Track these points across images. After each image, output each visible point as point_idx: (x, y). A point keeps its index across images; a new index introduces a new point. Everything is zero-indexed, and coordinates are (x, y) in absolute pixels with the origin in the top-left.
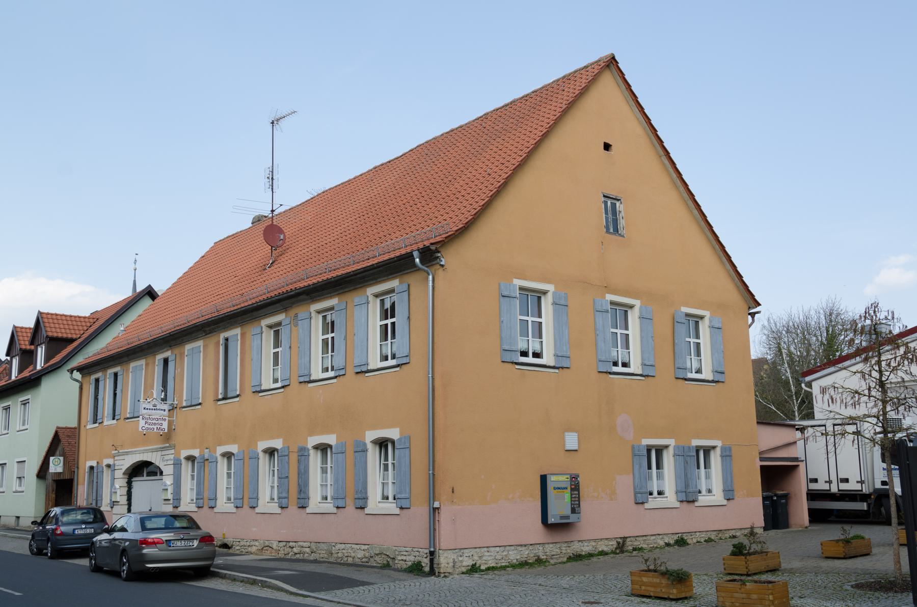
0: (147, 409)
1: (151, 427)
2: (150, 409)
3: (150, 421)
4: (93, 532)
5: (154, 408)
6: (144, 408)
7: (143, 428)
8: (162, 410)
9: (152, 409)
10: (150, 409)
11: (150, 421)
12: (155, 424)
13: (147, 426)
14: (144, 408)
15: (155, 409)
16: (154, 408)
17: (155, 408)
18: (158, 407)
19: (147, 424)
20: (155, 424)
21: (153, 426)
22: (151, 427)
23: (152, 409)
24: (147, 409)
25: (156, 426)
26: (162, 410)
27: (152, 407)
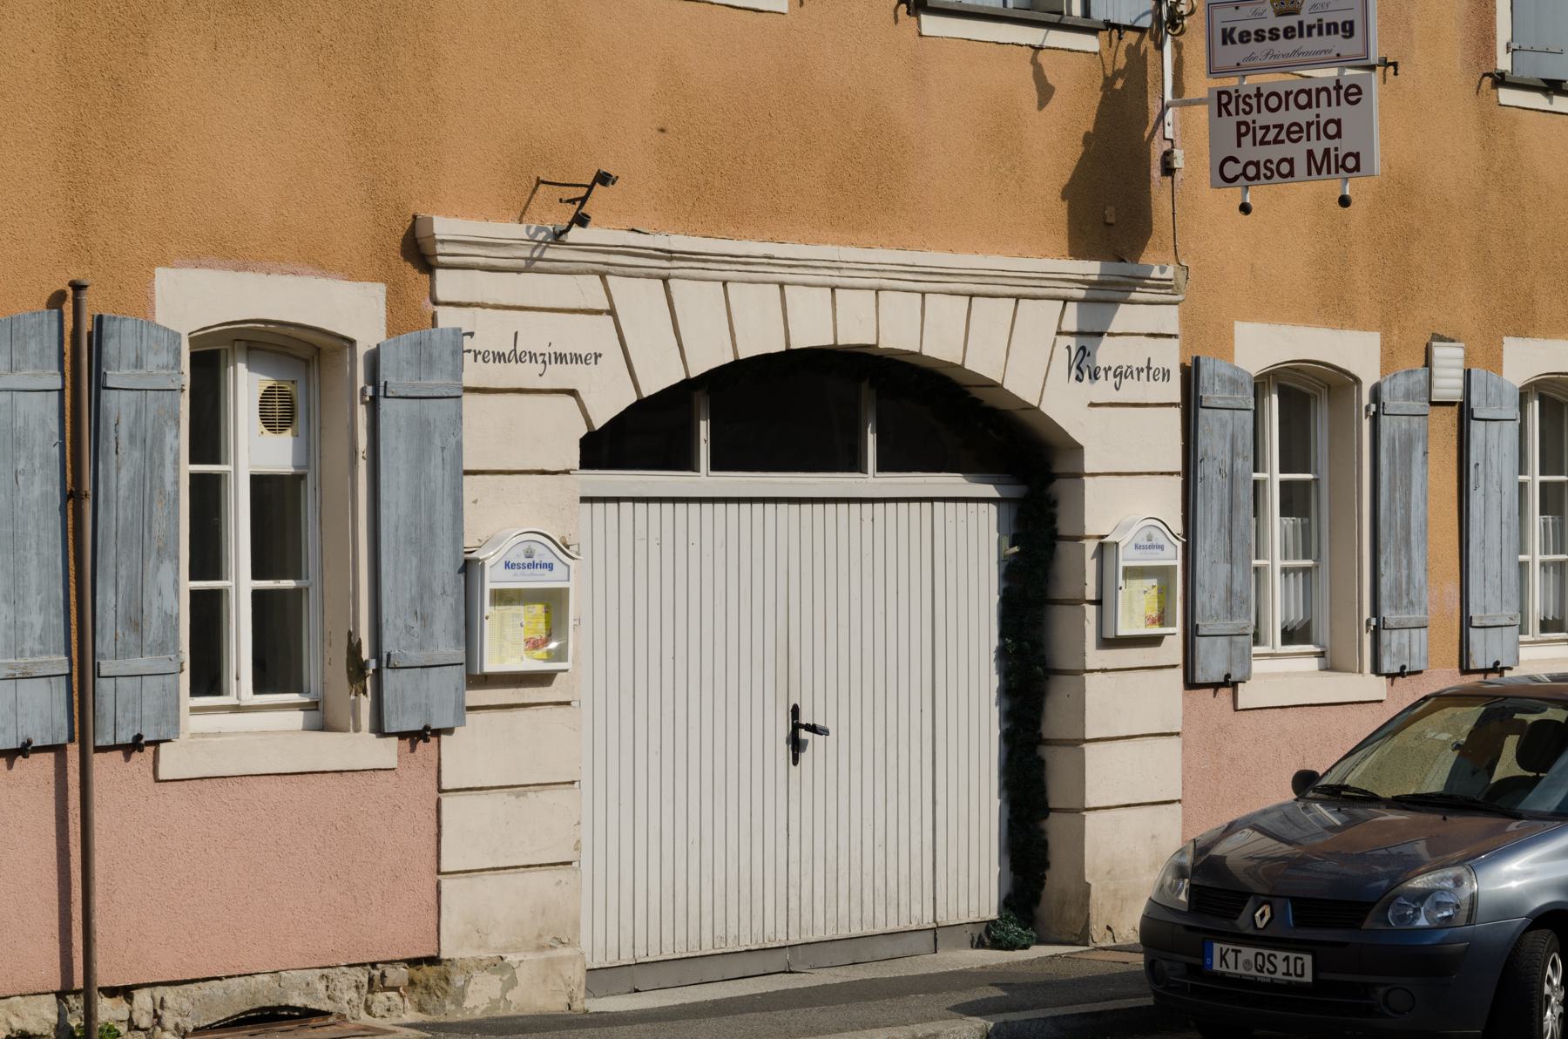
0: (1245, 37)
1: (1275, 153)
2: (1260, 35)
3: (1265, 118)
7: (1232, 170)
8: (1332, 28)
10: (1260, 35)
11: (1265, 118)
12: (1294, 132)
13: (1249, 151)
15: (1289, 34)
17: (1292, 21)
19: (1247, 140)
20: (1294, 132)
22: (1275, 153)
23: (1274, 33)
24: (1245, 37)
25: (1304, 146)
26: (1332, 28)
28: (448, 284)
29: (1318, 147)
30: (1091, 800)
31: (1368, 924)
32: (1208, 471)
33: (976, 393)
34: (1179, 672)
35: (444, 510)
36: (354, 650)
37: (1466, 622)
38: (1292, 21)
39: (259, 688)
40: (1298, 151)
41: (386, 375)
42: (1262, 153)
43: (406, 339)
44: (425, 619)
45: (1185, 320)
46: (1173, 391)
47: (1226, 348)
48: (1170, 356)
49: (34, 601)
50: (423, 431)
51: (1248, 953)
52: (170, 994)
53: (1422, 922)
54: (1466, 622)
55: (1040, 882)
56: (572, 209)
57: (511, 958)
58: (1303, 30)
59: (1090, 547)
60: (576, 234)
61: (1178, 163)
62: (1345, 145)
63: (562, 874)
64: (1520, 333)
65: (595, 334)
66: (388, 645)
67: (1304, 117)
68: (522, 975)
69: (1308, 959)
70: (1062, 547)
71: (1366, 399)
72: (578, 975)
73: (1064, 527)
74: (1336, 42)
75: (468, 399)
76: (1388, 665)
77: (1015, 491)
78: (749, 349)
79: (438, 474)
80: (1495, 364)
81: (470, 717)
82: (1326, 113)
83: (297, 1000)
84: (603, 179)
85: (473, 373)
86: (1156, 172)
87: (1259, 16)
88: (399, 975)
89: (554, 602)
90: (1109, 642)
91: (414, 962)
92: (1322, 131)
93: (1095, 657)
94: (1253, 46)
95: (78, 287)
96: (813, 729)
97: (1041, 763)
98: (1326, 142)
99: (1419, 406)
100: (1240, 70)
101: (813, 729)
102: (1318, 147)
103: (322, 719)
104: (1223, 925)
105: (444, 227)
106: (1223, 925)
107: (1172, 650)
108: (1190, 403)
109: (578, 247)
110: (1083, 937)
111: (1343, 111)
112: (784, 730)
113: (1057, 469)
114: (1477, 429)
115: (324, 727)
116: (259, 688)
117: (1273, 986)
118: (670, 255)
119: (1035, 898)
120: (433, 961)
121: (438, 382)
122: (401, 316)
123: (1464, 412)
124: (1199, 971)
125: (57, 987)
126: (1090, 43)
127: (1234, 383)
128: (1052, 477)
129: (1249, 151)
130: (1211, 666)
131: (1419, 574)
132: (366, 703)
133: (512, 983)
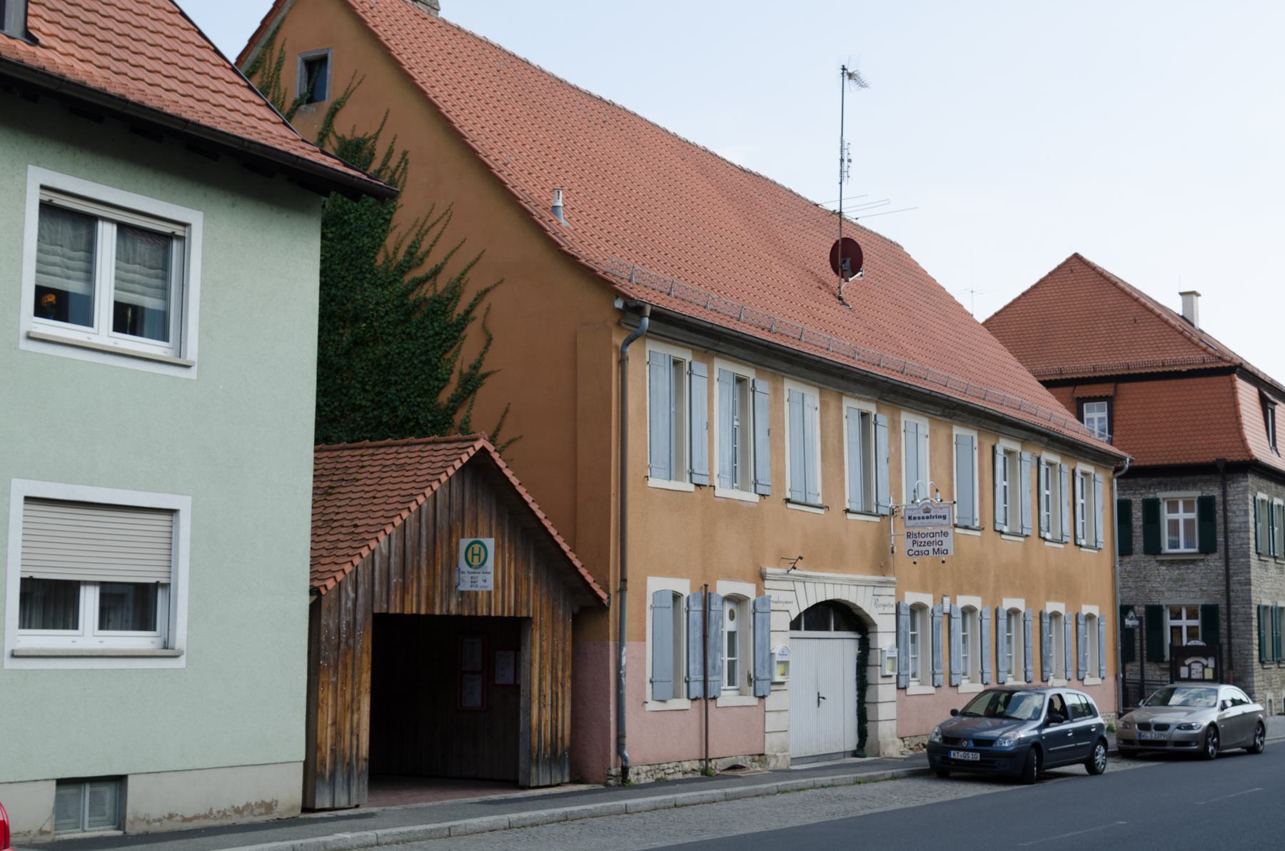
0: (915, 518)
1: (924, 549)
2: (919, 518)
3: (920, 539)
4: (978, 759)
5: (926, 515)
6: (910, 518)
7: (911, 553)
8: (940, 517)
9: (923, 518)
10: (919, 518)
11: (920, 539)
12: (929, 543)
13: (916, 548)
14: (910, 518)
15: (927, 518)
16: (926, 515)
17: (929, 515)
18: (933, 513)
19: (916, 545)
20: (929, 543)
21: (927, 548)
22: (924, 549)
23: (923, 518)
24: (915, 518)
25: (932, 547)
26: (940, 517)
27: (922, 514)
28: (767, 584)
29: (936, 548)
30: (880, 718)
31: (994, 745)
32: (901, 631)
33: (854, 611)
34: (895, 685)
35: (767, 639)
36: (749, 676)
37: (951, 673)
38: (929, 515)
39: (729, 685)
40: (930, 549)
41: (757, 607)
42: (919, 549)
43: (760, 597)
44: (764, 668)
45: (896, 592)
46: (893, 610)
47: (903, 600)
48: (893, 601)
49: (697, 662)
50: (763, 620)
51: (961, 753)
52: (718, 761)
53: (1007, 745)
54: (951, 673)
55: (865, 740)
56: (792, 566)
57: (778, 754)
58: (931, 517)
59: (879, 651)
60: (793, 571)
61: (895, 551)
62: (943, 547)
63: (785, 733)
64: (960, 594)
65: (790, 596)
66: (757, 675)
67: (932, 540)
68: (780, 759)
69: (978, 754)
70: (871, 652)
71: (930, 612)
72: (789, 759)
73: (871, 646)
74: (941, 520)
75: (772, 613)
76: (936, 685)
77: (858, 636)
78: (828, 599)
79: (766, 632)
80: (955, 603)
81: (772, 693)
82: (938, 539)
83: (740, 764)
84: (801, 558)
85: (773, 606)
86: (890, 553)
87: (919, 513)
88: (757, 758)
89: (786, 663)
90: (884, 677)
91: (760, 755)
92: (937, 543)
93: (880, 681)
94: (917, 520)
95: (706, 586)
96: (823, 698)
97: (865, 709)
98: (938, 547)
99: (941, 614)
100: (913, 526)
101: (823, 698)
102: (936, 548)
103: (741, 693)
104: (954, 746)
105: (769, 570)
106: (954, 746)
107: (894, 680)
108: (898, 614)
109: (791, 575)
110: (878, 755)
111: (943, 538)
112: (817, 698)
113: (870, 630)
114: (953, 620)
115: (741, 695)
116: (729, 685)
117: (969, 761)
118: (806, 576)
119: (864, 745)
120: (763, 754)
121: (766, 609)
122: (760, 592)
123: (950, 616)
124: (947, 760)
125: (699, 757)
126: (877, 519)
127: (906, 608)
128: (868, 633)
129: (916, 548)
130: (902, 685)
131: (941, 660)
132: (752, 688)
133: (777, 761)
